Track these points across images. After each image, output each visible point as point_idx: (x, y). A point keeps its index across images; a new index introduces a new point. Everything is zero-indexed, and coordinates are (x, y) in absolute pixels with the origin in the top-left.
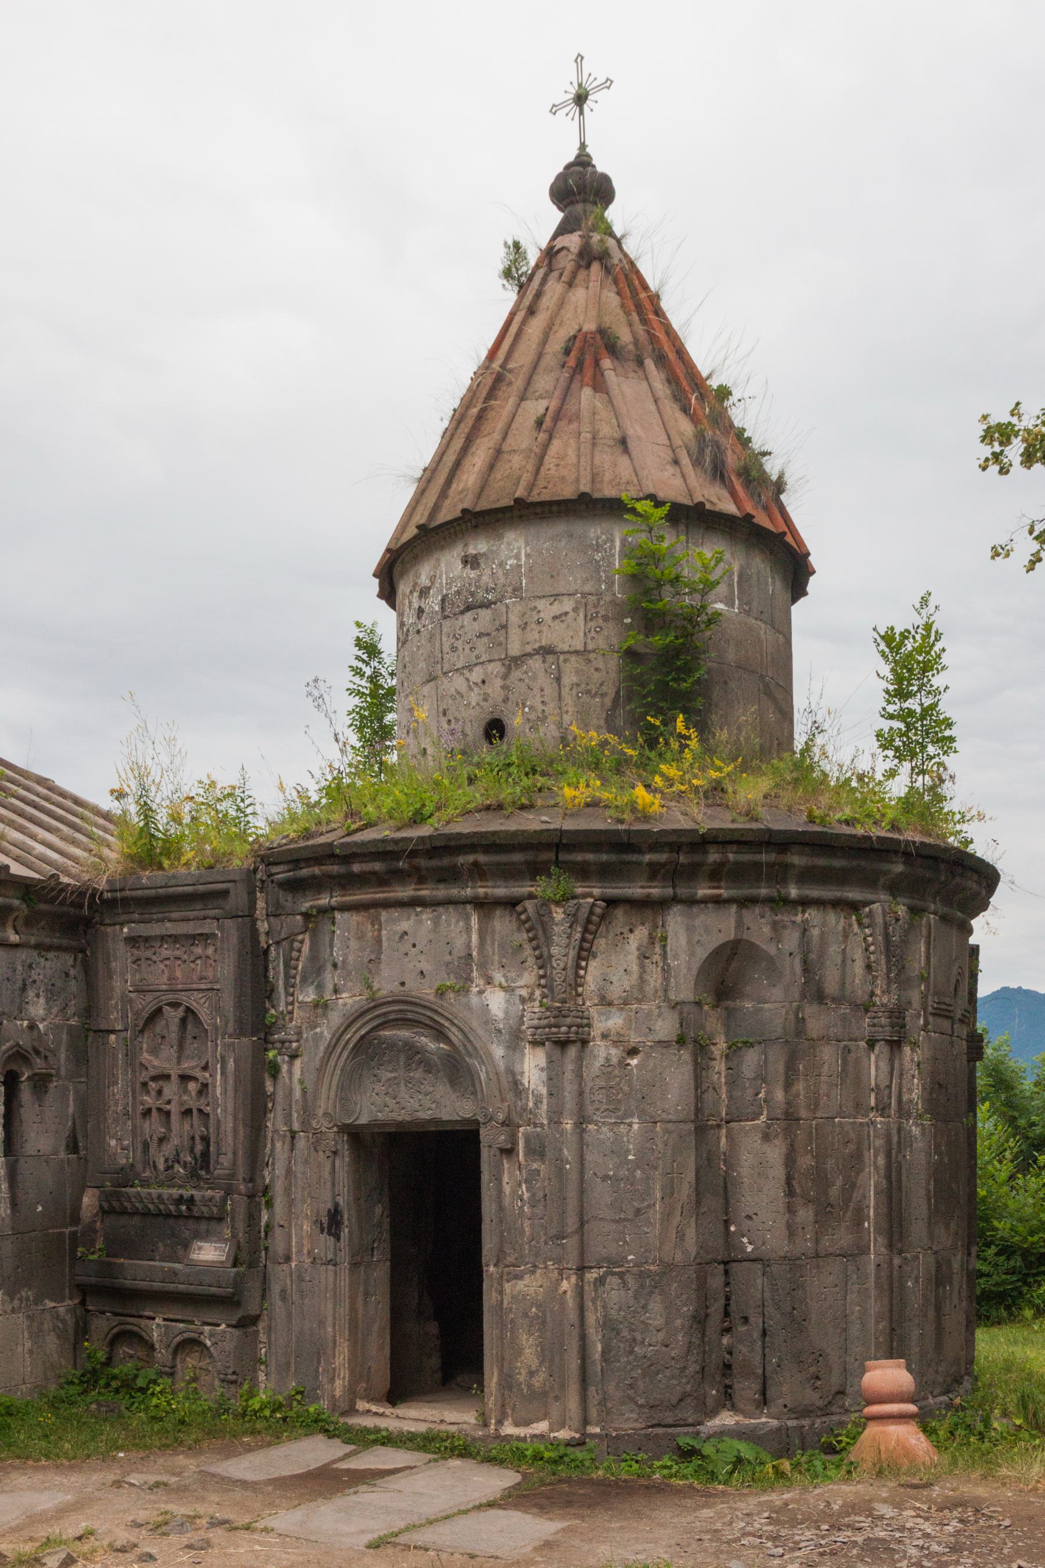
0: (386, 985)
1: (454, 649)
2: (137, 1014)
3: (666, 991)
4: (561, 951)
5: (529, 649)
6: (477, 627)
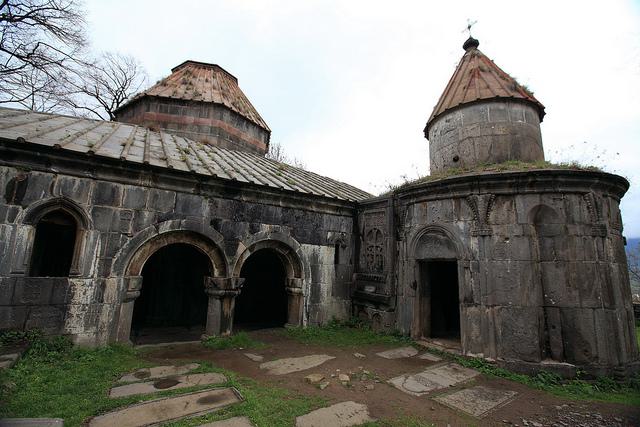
4: (481, 209)
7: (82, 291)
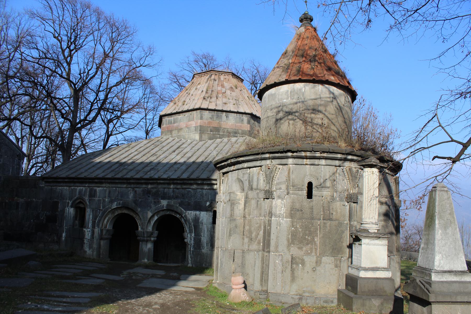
7: (88, 233)
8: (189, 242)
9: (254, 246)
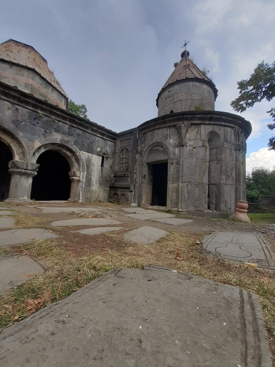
0: (154, 141)
1: (166, 103)
2: (120, 151)
3: (200, 138)
5: (177, 101)
6: (170, 100)
8: (81, 180)
9: (230, 182)
